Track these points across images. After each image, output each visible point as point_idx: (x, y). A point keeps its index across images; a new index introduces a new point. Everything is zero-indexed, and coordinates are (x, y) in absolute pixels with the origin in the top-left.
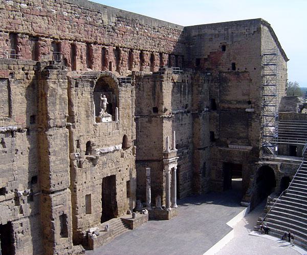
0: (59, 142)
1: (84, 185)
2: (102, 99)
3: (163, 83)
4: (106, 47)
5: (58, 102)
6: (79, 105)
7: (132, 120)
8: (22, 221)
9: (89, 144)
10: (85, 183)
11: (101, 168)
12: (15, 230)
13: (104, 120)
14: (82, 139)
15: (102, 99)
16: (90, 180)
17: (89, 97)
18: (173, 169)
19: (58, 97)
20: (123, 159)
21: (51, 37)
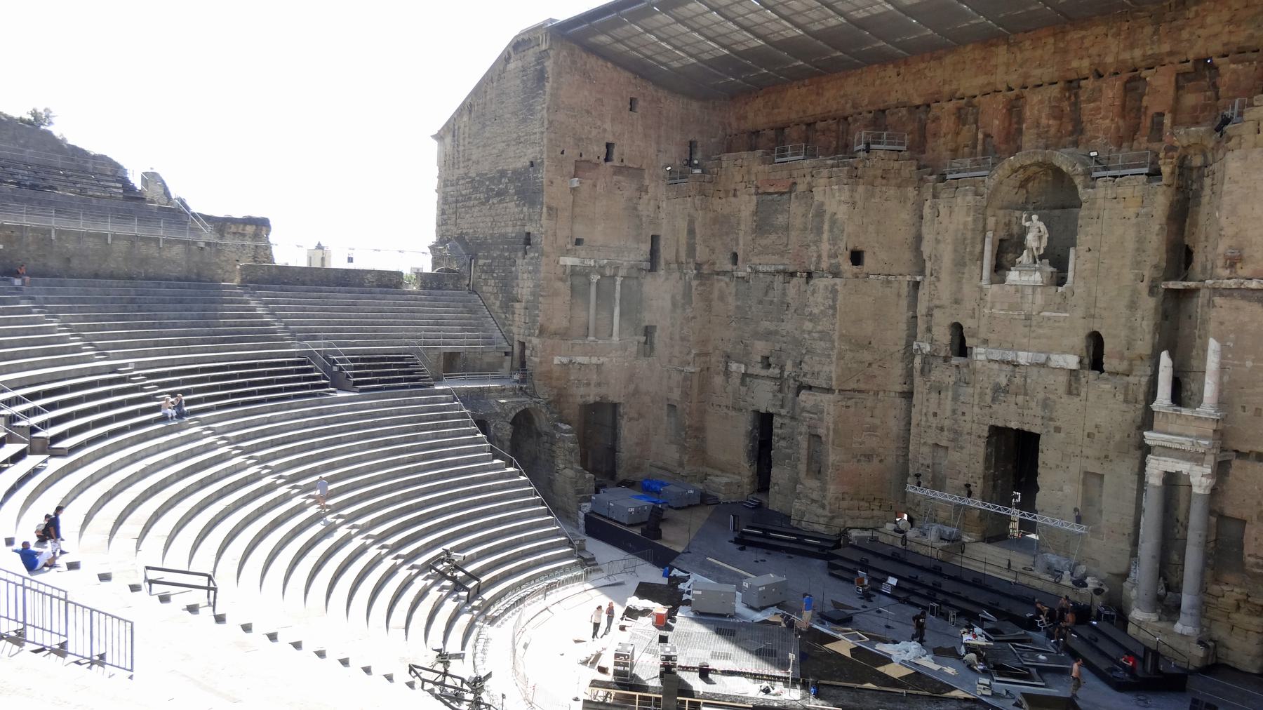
0: (820, 300)
1: (931, 418)
2: (1028, 224)
3: (1229, 155)
4: (1144, 73)
5: (826, 227)
6: (940, 237)
7: (1135, 292)
8: (787, 421)
9: (957, 329)
10: (935, 414)
11: (988, 399)
12: (775, 431)
13: (1013, 276)
14: (936, 313)
15: (1028, 224)
16: (948, 413)
17: (970, 219)
18: (1171, 480)
19: (827, 217)
20: (1077, 399)
21: (958, 95)
